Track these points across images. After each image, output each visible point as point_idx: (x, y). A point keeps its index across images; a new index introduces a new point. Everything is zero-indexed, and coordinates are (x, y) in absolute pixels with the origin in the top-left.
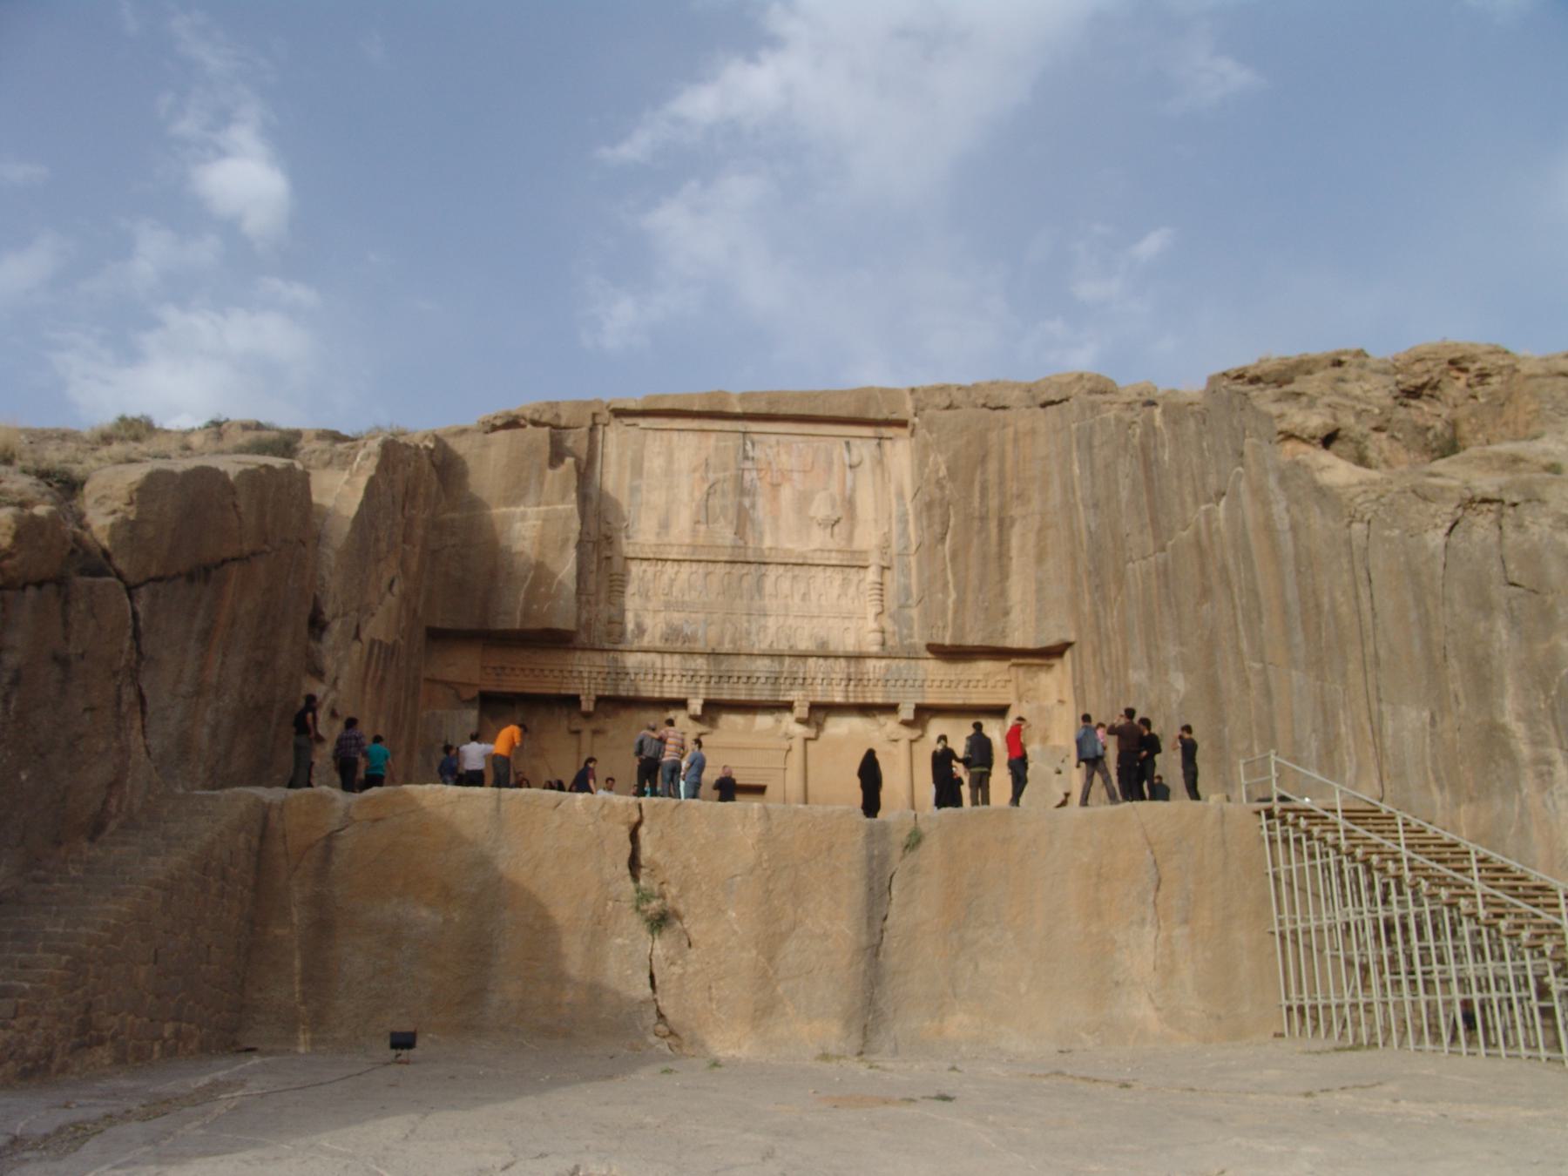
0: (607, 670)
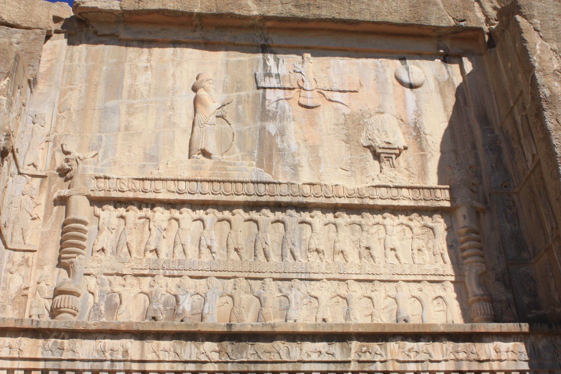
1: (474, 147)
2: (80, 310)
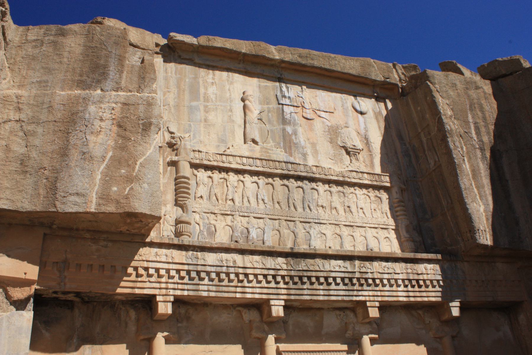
0: (186, 267)
1: (396, 153)
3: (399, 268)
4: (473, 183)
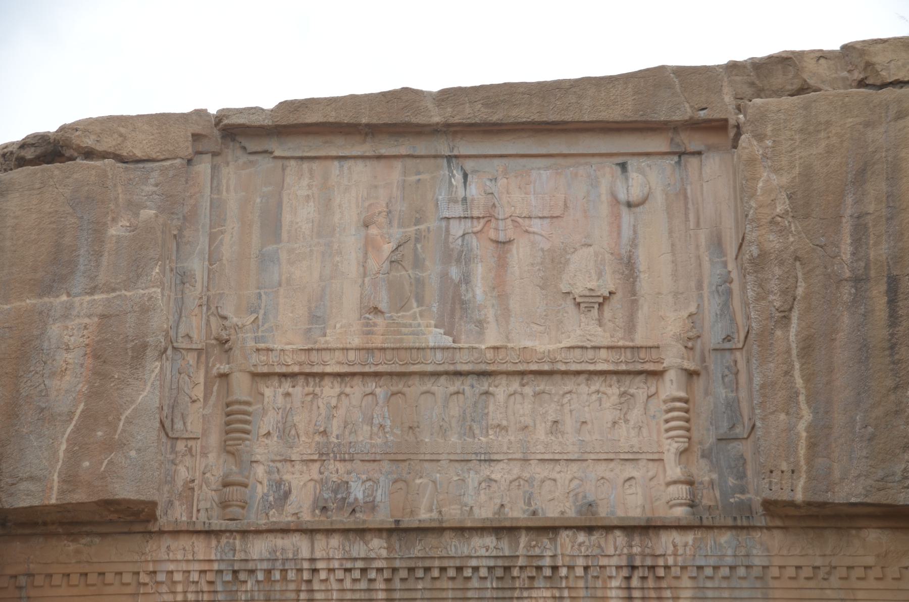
1: (700, 286)
2: (248, 501)
3: (613, 546)
4: (797, 366)
